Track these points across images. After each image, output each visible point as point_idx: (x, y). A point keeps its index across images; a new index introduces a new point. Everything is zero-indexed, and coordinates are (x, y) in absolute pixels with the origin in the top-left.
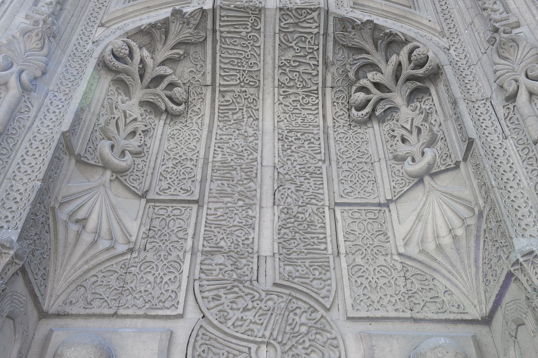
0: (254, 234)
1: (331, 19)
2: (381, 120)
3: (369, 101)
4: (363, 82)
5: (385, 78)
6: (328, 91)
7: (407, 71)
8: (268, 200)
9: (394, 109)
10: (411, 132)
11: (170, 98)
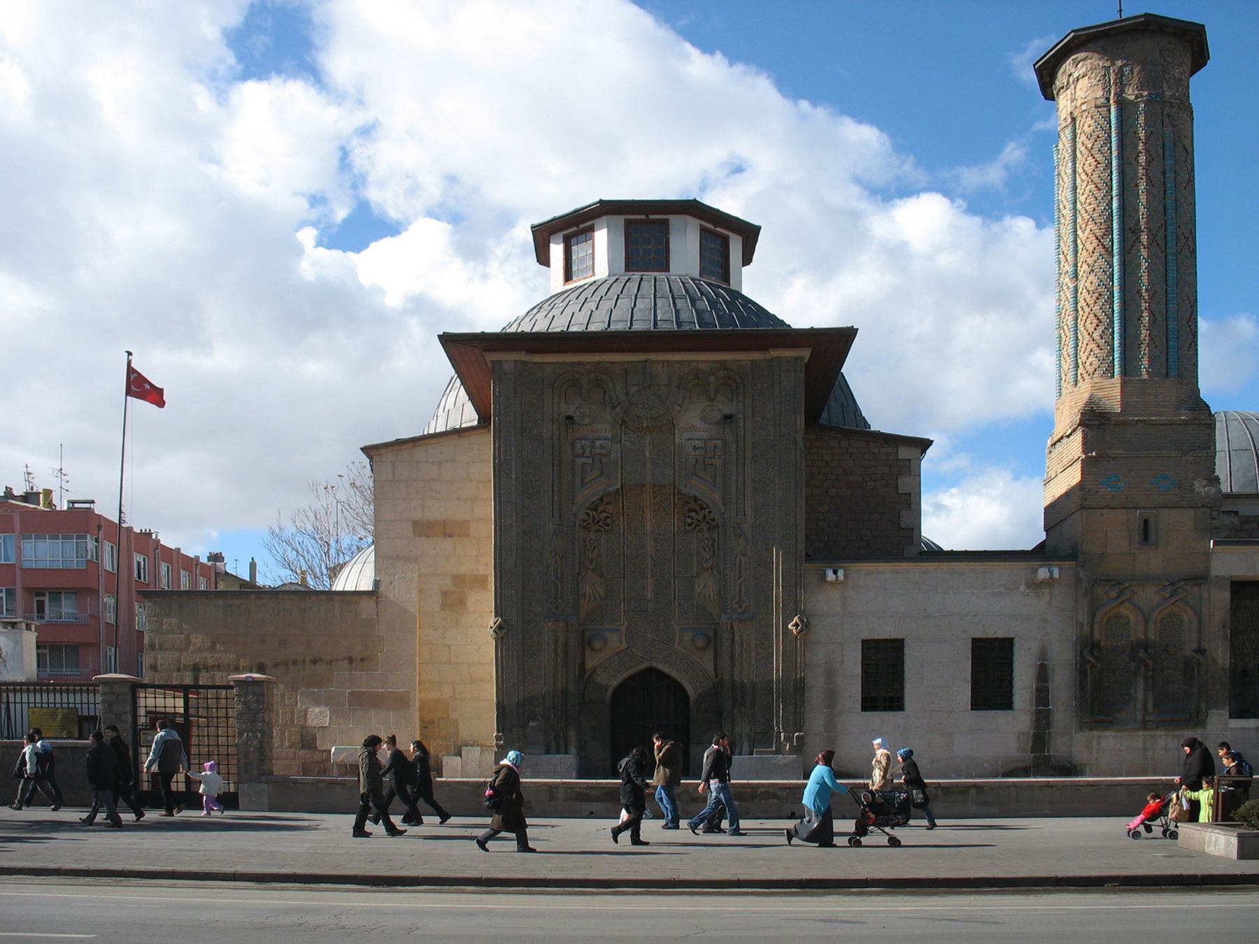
0: (645, 592)
1: (676, 490)
2: (699, 531)
3: (692, 523)
4: (690, 514)
5: (700, 518)
6: (676, 515)
7: (707, 520)
8: (649, 576)
9: (701, 531)
10: (707, 546)
11: (605, 524)
